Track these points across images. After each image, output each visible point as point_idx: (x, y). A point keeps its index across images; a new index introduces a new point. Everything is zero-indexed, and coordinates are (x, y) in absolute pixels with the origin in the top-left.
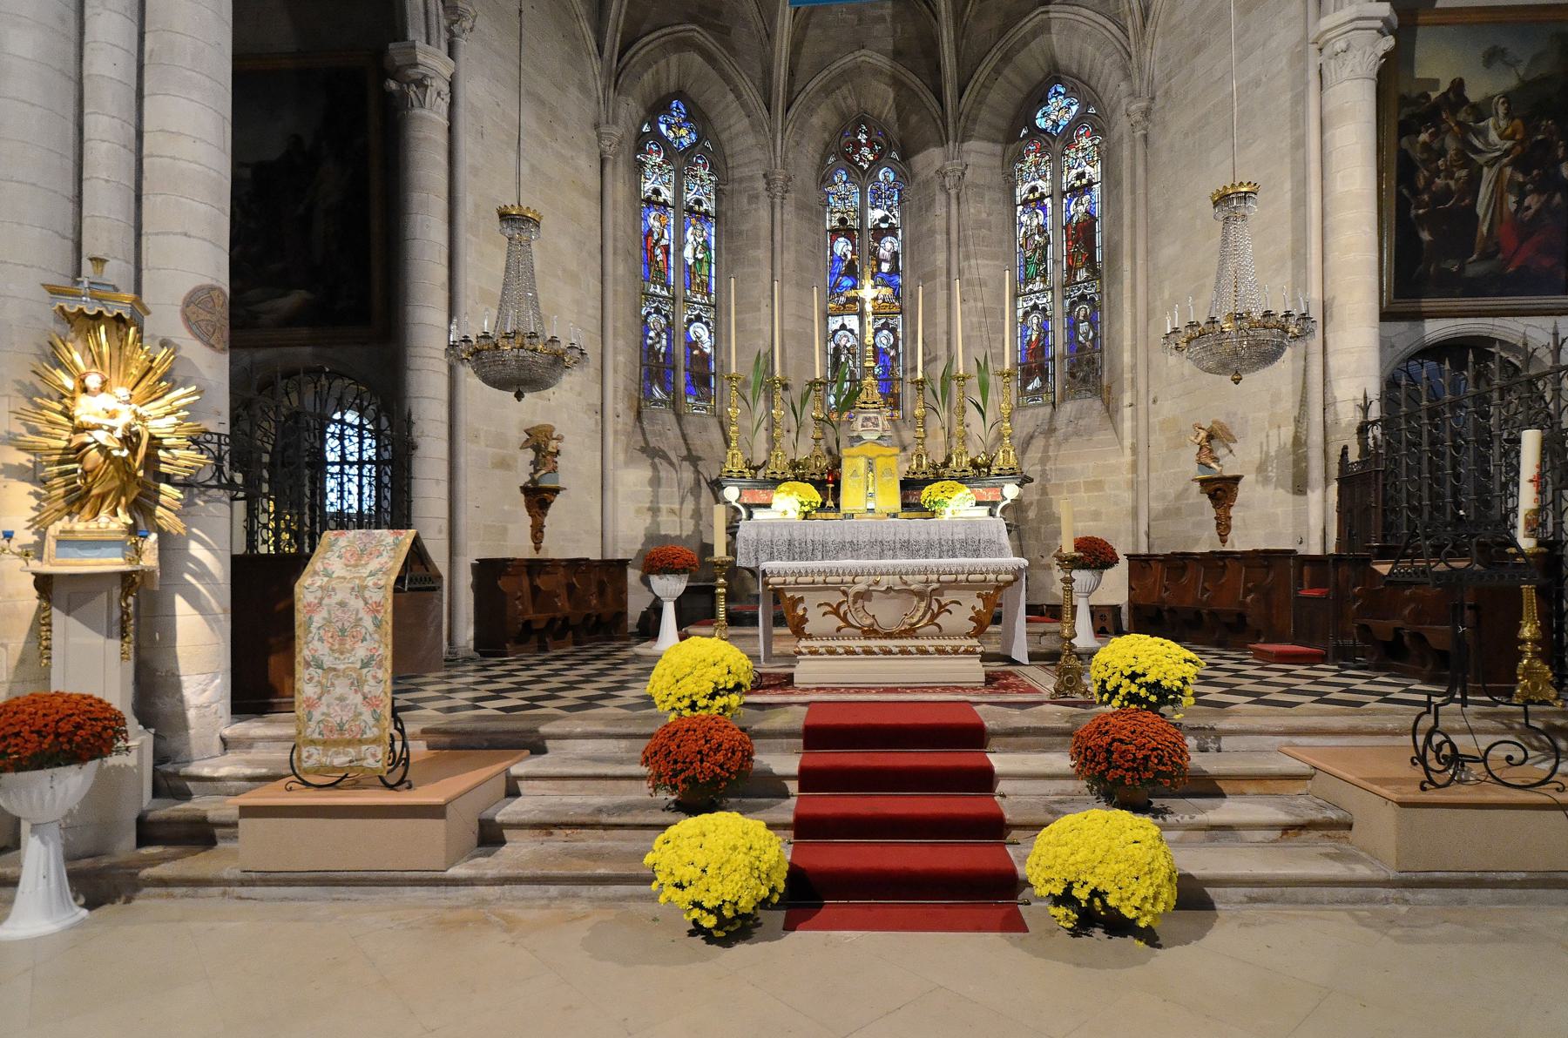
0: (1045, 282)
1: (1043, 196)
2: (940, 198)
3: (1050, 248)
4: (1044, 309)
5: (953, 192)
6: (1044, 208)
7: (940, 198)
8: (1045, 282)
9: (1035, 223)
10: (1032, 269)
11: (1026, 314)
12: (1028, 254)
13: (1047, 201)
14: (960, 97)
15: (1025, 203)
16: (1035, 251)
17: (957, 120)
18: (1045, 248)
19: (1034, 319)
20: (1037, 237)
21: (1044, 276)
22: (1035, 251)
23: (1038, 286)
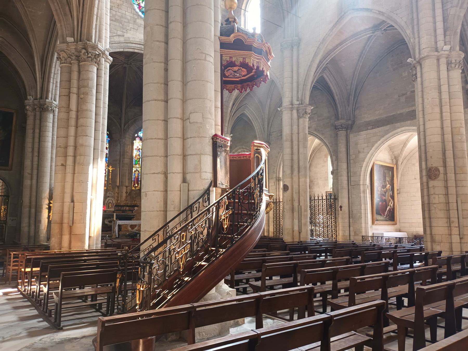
0: (139, 166)
1: (139, 149)
2: (119, 145)
3: (141, 159)
4: (139, 171)
5: (122, 145)
6: (140, 151)
7: (119, 145)
8: (139, 166)
9: (138, 154)
10: (137, 162)
11: (135, 171)
12: (136, 159)
13: (141, 150)
14: (125, 126)
15: (136, 149)
16: (137, 159)
17: (124, 131)
18: (139, 159)
19: (137, 172)
20: (138, 157)
21: (139, 164)
22: (137, 159)
23: (138, 166)
